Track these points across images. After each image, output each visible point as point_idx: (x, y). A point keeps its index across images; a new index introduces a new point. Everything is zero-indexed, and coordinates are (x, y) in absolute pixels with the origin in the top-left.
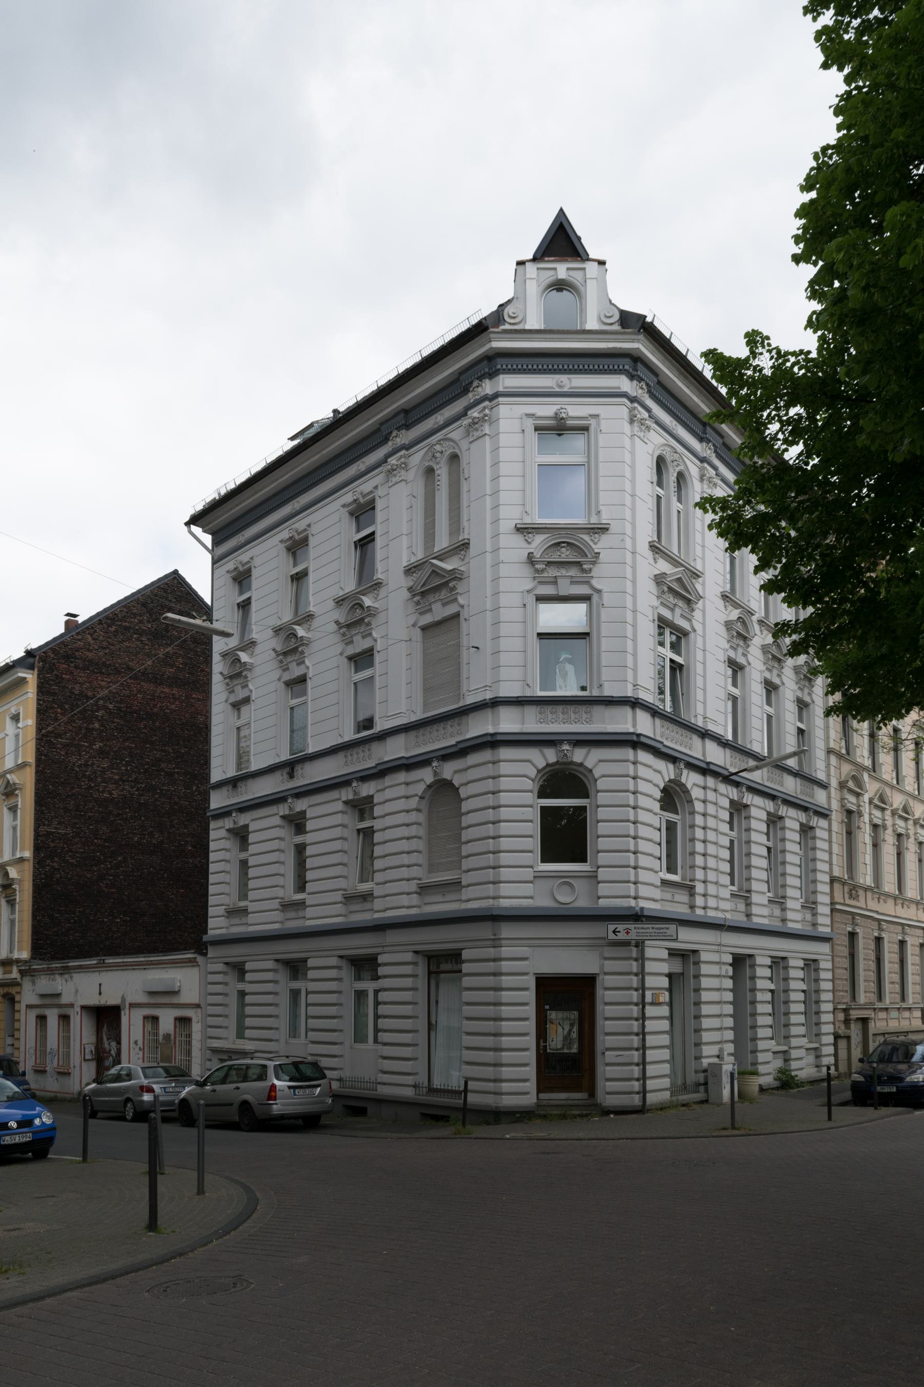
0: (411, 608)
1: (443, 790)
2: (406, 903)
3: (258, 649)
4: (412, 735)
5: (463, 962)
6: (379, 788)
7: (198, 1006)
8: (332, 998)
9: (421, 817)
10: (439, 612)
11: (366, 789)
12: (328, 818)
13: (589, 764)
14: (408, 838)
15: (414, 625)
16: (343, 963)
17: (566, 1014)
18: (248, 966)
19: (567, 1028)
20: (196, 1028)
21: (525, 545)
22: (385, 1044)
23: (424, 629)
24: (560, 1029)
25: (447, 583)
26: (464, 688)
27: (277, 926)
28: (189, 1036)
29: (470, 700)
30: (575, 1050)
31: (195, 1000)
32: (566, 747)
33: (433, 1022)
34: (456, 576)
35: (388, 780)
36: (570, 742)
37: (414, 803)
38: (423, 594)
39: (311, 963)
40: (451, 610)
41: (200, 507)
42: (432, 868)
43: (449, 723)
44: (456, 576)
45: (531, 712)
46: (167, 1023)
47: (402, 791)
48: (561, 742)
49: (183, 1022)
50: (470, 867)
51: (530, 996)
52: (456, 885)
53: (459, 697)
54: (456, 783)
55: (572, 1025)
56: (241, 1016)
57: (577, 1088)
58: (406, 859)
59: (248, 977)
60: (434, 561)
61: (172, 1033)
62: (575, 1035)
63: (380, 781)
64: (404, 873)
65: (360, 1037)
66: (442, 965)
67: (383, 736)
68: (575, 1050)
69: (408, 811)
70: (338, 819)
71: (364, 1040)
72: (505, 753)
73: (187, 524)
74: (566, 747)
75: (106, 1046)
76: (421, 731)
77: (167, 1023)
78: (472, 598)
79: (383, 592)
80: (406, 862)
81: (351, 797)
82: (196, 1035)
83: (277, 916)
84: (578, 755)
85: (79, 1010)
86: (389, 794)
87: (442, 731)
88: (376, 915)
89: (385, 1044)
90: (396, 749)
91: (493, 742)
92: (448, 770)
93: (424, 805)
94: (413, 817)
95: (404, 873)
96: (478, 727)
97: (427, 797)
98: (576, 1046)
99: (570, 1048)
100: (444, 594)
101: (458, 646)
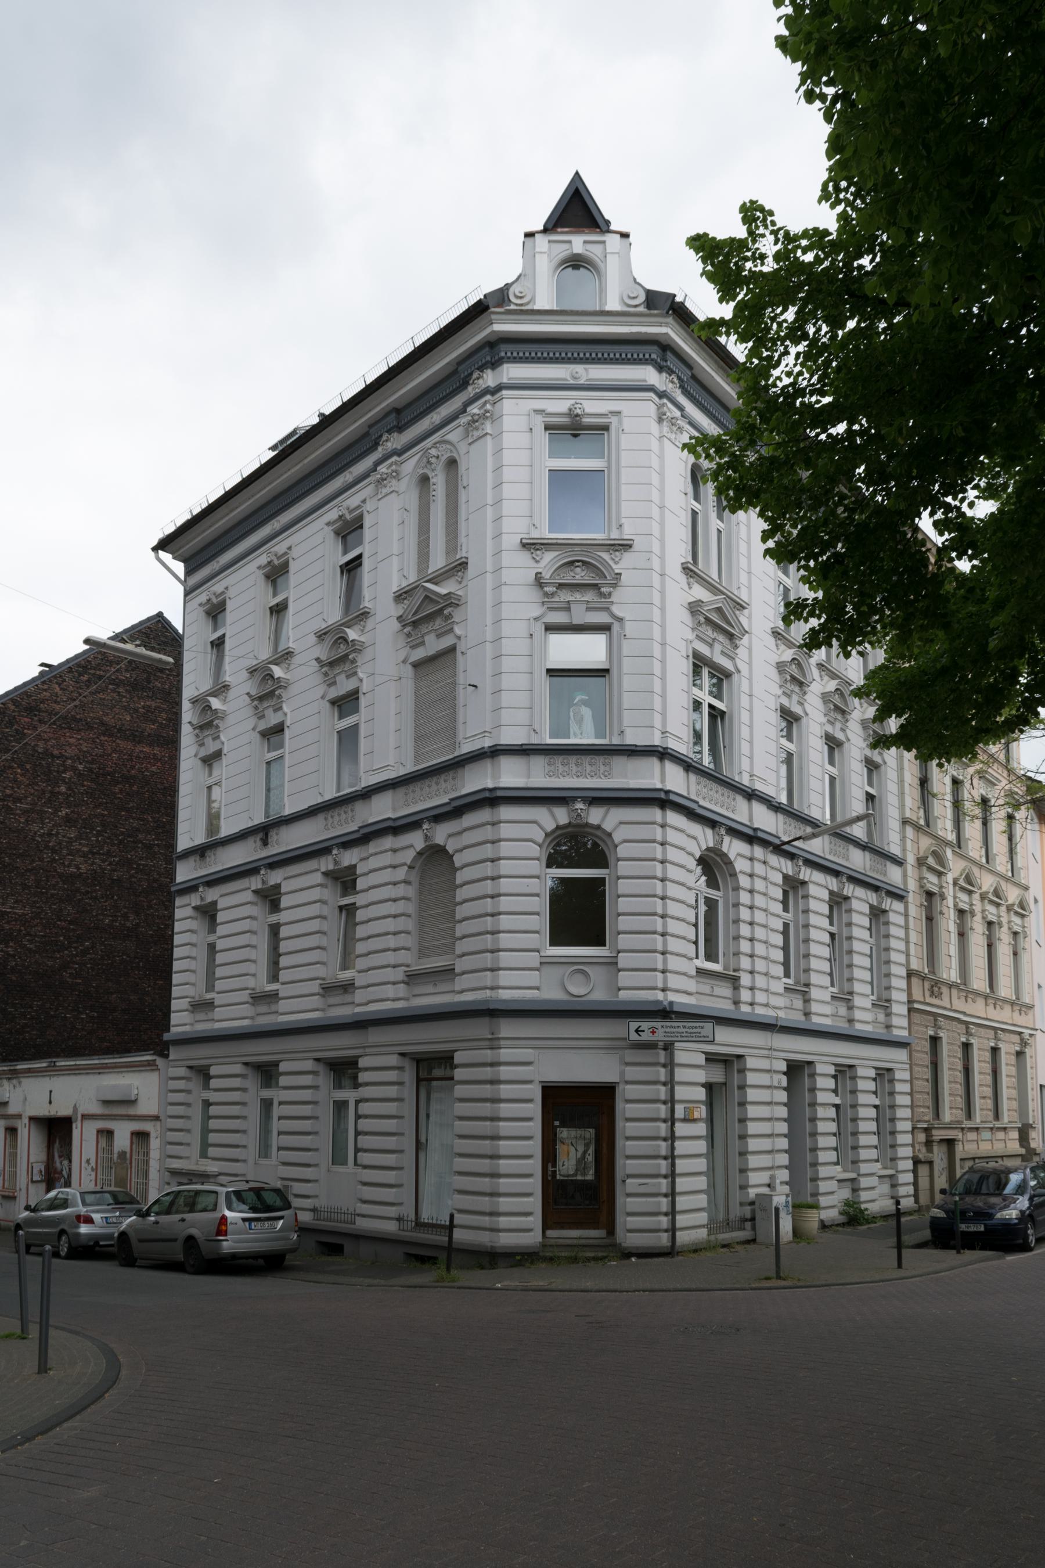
0: (402, 641)
1: (436, 856)
2: (391, 995)
4: (401, 792)
5: (456, 1067)
6: (364, 855)
7: (157, 1118)
8: (306, 1110)
9: (410, 891)
10: (433, 645)
11: (349, 858)
12: (305, 890)
13: (607, 826)
14: (395, 916)
15: (404, 662)
16: (320, 1068)
17: (580, 1132)
18: (213, 1071)
19: (581, 1149)
20: (155, 1143)
22: (365, 1167)
23: (416, 665)
24: (572, 1149)
25: (441, 610)
26: (460, 736)
27: (246, 1022)
28: (147, 1154)
29: (466, 748)
30: (590, 1176)
31: (153, 1111)
32: (579, 805)
33: (423, 1139)
34: (452, 602)
35: (373, 847)
36: (584, 799)
37: (401, 874)
38: (415, 624)
39: (283, 1067)
40: (446, 642)
41: (170, 529)
42: (423, 952)
43: (443, 776)
44: (452, 602)
45: (538, 763)
47: (388, 859)
48: (574, 799)
50: (465, 950)
51: (535, 1109)
52: (448, 973)
53: (454, 745)
54: (450, 849)
55: (587, 1146)
56: (206, 1131)
57: (594, 1225)
58: (391, 942)
59: (214, 1083)
60: (428, 585)
61: (128, 1150)
62: (590, 1158)
63: (364, 848)
64: (390, 958)
65: (338, 1157)
66: (432, 1069)
67: (367, 794)
68: (590, 1176)
69: (395, 884)
70: (316, 894)
71: (345, 1163)
72: (506, 812)
73: (155, 549)
74: (579, 805)
75: (58, 1165)
76: (411, 787)
78: (470, 627)
79: (370, 623)
80: (392, 945)
81: (331, 867)
82: (155, 1154)
84: (595, 816)
85: (26, 1121)
86: (374, 863)
88: (358, 1010)
89: (365, 1167)
90: (383, 809)
91: (492, 799)
92: (441, 833)
93: (414, 877)
94: (401, 891)
95: (390, 958)
96: (476, 780)
97: (418, 865)
98: (592, 1172)
99: (584, 1174)
100: (438, 623)
101: (454, 684)
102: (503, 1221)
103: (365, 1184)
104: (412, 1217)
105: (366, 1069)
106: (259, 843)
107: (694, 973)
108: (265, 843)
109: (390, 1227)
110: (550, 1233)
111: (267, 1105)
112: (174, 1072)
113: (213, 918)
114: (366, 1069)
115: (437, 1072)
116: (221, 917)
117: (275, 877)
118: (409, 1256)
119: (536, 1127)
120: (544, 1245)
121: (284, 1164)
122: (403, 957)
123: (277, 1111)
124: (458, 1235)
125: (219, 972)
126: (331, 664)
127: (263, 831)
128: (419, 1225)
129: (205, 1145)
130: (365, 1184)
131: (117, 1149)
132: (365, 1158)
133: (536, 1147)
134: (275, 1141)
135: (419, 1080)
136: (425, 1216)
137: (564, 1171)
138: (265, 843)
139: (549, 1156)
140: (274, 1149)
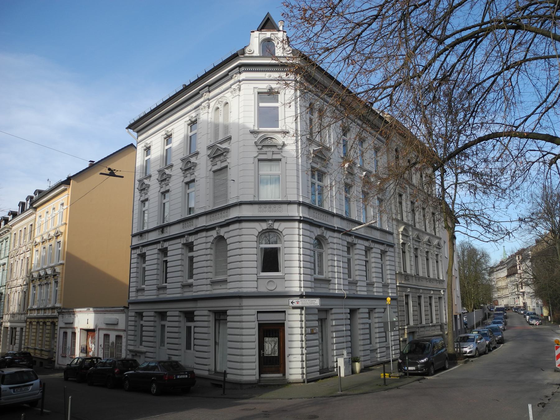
0: (210, 163)
1: (220, 239)
2: (205, 289)
3: (152, 178)
4: (209, 216)
5: (228, 316)
6: (196, 238)
7: (125, 331)
8: (176, 330)
9: (212, 252)
11: (191, 239)
12: (175, 249)
13: (280, 229)
14: (207, 261)
15: (210, 170)
16: (182, 315)
17: (273, 339)
18: (144, 314)
19: (273, 345)
20: (124, 340)
21: (254, 138)
22: (197, 351)
23: (214, 172)
24: (270, 345)
25: (222, 154)
26: (229, 198)
27: (155, 297)
28: (121, 343)
30: (277, 355)
31: (124, 328)
32: (270, 222)
33: (217, 341)
34: (227, 151)
35: (199, 235)
36: (272, 220)
37: (209, 245)
39: (168, 314)
40: (224, 165)
41: (132, 122)
42: (217, 274)
43: (223, 212)
44: (227, 151)
46: (112, 339)
47: (203, 240)
48: (269, 220)
49: (119, 337)
50: (231, 274)
51: (256, 331)
52: (225, 281)
53: (227, 200)
54: (225, 237)
55: (275, 344)
56: (142, 336)
57: (278, 372)
58: (205, 270)
59: (144, 318)
60: (218, 145)
61: (115, 342)
62: (276, 348)
63: (196, 236)
64: (205, 276)
65: (188, 347)
66: (220, 316)
67: (197, 217)
68: (277, 355)
69: (206, 249)
70: (179, 251)
71: (190, 349)
72: (244, 225)
73: (127, 128)
74: (270, 222)
76: (212, 215)
77: (112, 339)
78: (232, 160)
79: (199, 156)
80: (206, 271)
81: (185, 242)
82: (124, 344)
83: (155, 292)
84: (276, 225)
86: (199, 241)
87: (220, 215)
88: (194, 294)
89: (197, 351)
90: (202, 222)
91: (239, 220)
92: (222, 231)
93: (213, 247)
94: (208, 251)
95: (205, 276)
96: (234, 213)
97: (215, 242)
98: (277, 353)
99: (274, 354)
100: (222, 158)
101: (226, 180)
102: (245, 372)
103: (197, 357)
104: (213, 370)
105: (197, 316)
106: (160, 232)
107: (313, 280)
108: (162, 232)
109: (206, 373)
110: (262, 375)
111: (163, 326)
112: (130, 314)
113: (145, 258)
114: (197, 316)
115: (222, 317)
116: (147, 258)
117: (166, 245)
118: (213, 384)
119: (257, 337)
120: (259, 381)
121: (169, 349)
122: (210, 275)
123: (167, 329)
124: (229, 377)
125: (146, 278)
126: (186, 170)
127: (162, 228)
128: (216, 372)
129: (141, 341)
130: (197, 357)
131: (111, 341)
132: (197, 348)
133: (256, 345)
134: (167, 340)
135: (216, 320)
136: (218, 369)
137: (267, 353)
138: (162, 232)
139: (261, 347)
140: (166, 343)
